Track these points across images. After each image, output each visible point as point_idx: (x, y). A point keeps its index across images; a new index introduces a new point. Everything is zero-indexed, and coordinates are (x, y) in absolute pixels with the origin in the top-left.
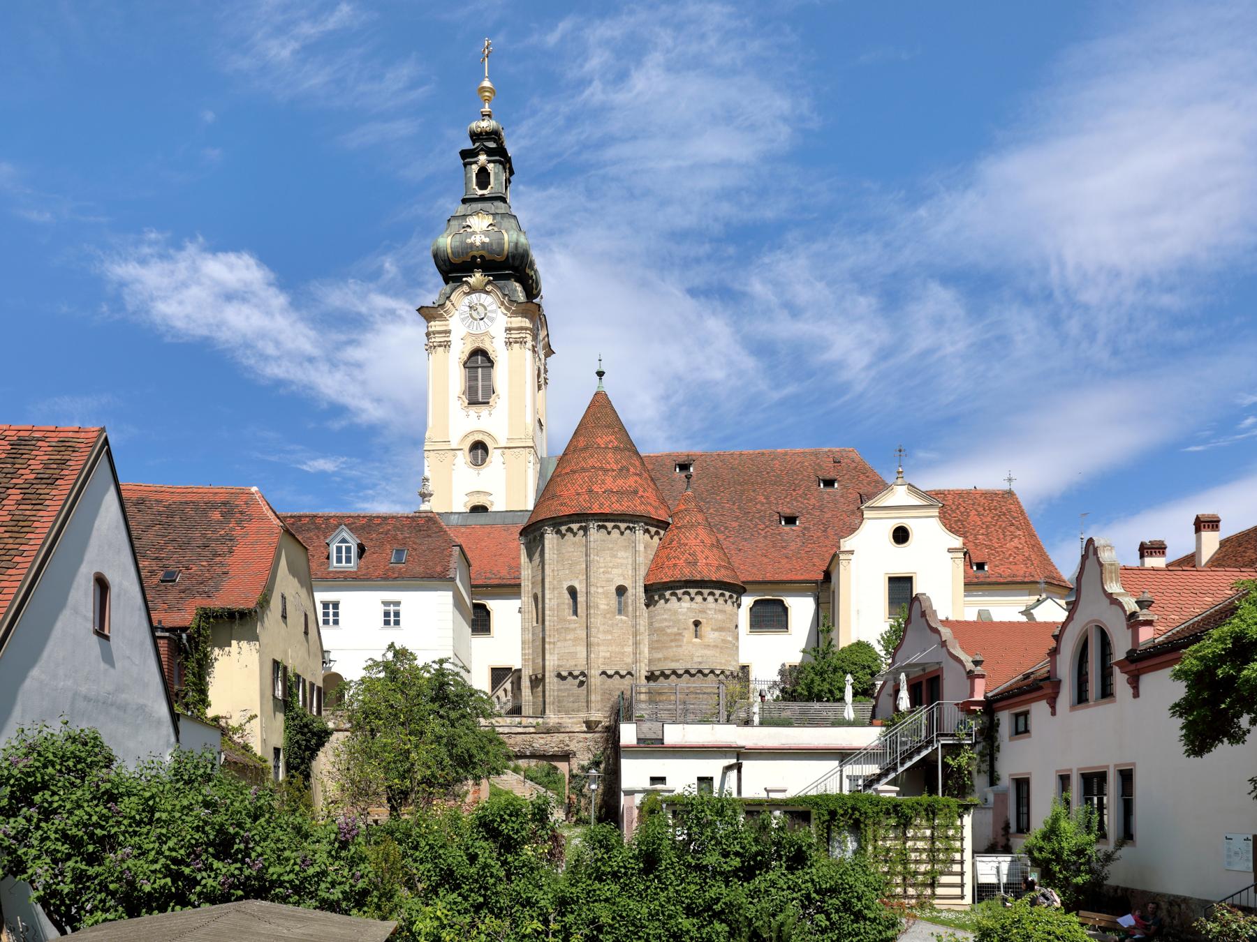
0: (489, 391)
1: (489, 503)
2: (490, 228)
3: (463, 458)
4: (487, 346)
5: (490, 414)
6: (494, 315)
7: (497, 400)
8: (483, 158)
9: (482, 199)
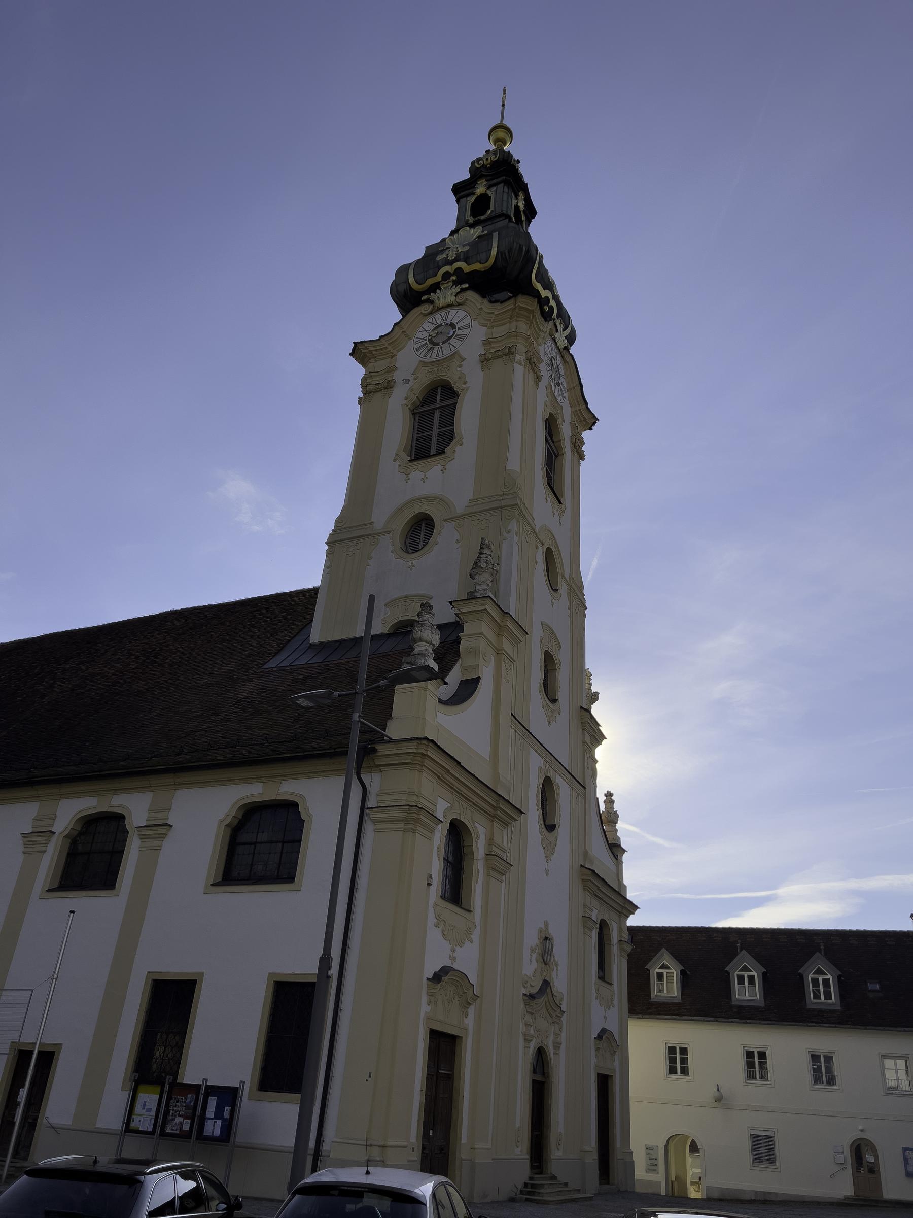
0: (448, 436)
5: (443, 471)
6: (466, 331)
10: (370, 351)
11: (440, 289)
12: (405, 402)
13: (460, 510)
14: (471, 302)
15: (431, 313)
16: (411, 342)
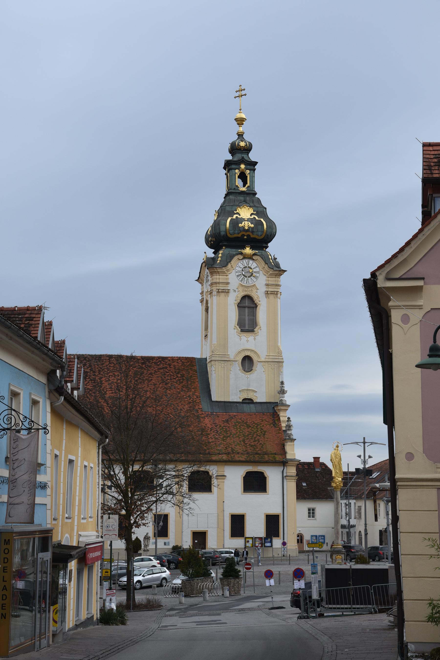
1: (255, 397)
2: (253, 216)
3: (237, 366)
4: (254, 295)
5: (255, 339)
6: (258, 275)
7: (259, 331)
9: (243, 193)
10: (218, 271)
11: (246, 248)
12: (235, 302)
13: (263, 359)
14: (259, 260)
15: (242, 259)
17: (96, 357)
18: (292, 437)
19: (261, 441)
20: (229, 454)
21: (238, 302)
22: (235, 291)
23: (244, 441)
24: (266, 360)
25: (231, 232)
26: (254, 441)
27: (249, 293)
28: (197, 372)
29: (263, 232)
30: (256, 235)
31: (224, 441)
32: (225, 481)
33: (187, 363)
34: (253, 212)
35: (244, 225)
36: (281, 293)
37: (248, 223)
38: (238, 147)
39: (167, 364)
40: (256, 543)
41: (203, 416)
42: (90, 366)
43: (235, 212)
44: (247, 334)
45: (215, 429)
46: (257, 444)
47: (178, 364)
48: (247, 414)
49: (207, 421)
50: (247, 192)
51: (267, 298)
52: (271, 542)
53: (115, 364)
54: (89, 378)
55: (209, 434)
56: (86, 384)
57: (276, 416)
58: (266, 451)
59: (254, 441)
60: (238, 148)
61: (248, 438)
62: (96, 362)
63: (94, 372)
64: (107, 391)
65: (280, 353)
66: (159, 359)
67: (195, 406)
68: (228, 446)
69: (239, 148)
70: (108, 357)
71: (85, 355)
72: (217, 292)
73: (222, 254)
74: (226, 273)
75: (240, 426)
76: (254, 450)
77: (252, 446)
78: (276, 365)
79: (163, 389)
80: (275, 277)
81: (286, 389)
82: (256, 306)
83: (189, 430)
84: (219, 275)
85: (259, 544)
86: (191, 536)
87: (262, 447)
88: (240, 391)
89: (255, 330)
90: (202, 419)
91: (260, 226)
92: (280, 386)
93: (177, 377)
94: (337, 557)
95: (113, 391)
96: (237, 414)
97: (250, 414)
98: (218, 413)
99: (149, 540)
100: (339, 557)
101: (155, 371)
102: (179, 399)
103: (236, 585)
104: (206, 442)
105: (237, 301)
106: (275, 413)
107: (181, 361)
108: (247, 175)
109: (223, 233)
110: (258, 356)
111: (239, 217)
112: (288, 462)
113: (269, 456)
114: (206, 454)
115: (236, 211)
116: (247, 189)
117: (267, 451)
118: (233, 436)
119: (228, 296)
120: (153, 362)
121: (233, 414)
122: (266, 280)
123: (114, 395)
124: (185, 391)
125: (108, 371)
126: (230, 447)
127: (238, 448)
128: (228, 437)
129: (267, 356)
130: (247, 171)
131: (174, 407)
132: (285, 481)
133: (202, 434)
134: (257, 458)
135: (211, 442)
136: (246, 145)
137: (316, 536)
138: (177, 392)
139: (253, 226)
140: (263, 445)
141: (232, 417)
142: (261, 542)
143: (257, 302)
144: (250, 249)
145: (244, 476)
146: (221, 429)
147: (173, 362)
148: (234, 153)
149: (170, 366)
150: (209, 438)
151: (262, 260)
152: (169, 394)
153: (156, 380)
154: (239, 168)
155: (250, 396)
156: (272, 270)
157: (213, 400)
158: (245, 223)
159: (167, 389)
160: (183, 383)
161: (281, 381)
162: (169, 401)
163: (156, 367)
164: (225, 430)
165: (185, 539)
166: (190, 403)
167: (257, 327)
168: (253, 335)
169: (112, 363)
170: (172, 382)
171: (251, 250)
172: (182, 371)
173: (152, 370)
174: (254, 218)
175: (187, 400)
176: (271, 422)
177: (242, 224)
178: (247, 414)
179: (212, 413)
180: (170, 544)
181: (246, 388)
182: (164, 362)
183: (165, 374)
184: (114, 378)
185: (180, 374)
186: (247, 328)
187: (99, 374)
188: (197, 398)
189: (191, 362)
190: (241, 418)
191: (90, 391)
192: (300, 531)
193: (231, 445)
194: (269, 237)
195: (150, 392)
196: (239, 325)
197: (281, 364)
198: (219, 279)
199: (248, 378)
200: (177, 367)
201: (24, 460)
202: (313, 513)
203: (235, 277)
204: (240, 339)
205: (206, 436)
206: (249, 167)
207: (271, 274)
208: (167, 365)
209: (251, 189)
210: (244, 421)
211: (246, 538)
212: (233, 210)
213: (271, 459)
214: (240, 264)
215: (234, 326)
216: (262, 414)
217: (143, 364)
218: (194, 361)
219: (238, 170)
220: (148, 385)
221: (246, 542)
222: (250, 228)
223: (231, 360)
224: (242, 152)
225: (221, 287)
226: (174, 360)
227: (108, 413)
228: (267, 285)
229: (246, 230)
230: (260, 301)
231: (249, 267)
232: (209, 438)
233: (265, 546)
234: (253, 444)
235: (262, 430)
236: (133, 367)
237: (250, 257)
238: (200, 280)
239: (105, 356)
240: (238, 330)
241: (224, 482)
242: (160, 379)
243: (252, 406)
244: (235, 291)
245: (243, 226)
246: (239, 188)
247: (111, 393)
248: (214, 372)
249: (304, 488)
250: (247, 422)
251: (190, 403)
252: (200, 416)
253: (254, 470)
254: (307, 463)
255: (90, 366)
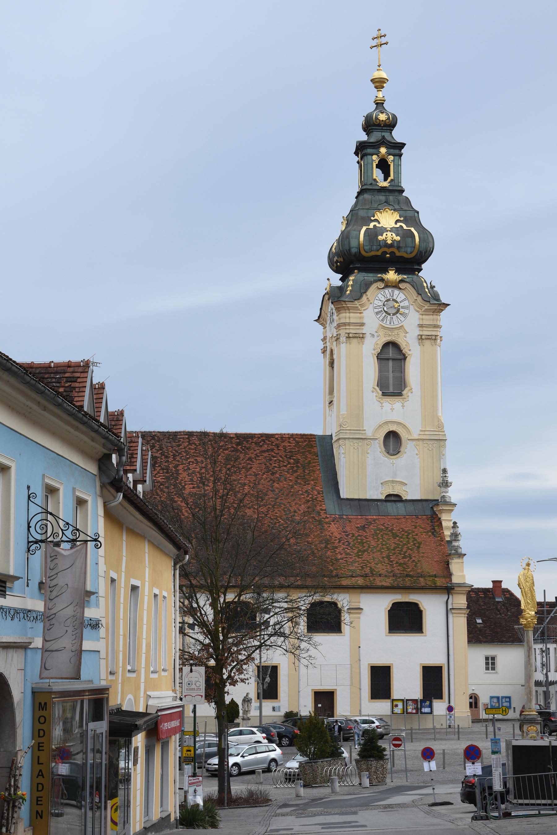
3: (378, 447)
5: (403, 406)
6: (407, 311)
7: (410, 394)
8: (383, 150)
10: (348, 307)
11: (388, 272)
12: (373, 352)
13: (415, 436)
16: (371, 306)
17: (170, 435)
18: (459, 551)
19: (414, 557)
20: (366, 576)
21: (378, 352)
22: (373, 335)
23: (388, 557)
24: (420, 438)
25: (366, 248)
26: (403, 558)
27: (394, 339)
28: (317, 456)
29: (414, 247)
30: (404, 252)
31: (359, 558)
32: (361, 616)
33: (302, 442)
34: (399, 218)
35: (386, 238)
36: (441, 337)
37: (392, 235)
38: (377, 122)
39: (273, 444)
40: (408, 707)
41: (327, 520)
42: (161, 448)
43: (372, 218)
44: (391, 400)
45: (346, 540)
46: (408, 561)
47: (289, 444)
48: (392, 517)
49: (333, 528)
50: (390, 188)
51: (421, 345)
52: (431, 706)
53: (197, 446)
54: (159, 466)
55: (336, 547)
56: (156, 475)
57: (435, 521)
58: (422, 572)
59: (403, 558)
60: (375, 123)
61: (395, 553)
62: (170, 442)
63: (167, 457)
64: (185, 485)
65: (440, 427)
66: (261, 437)
67: (316, 506)
68: (365, 565)
69: (377, 124)
70: (186, 435)
71: (154, 432)
72: (347, 337)
73: (353, 280)
74: (359, 310)
75: (382, 536)
76: (403, 571)
77: (400, 565)
78: (434, 445)
79: (268, 482)
80: (433, 315)
81: (450, 480)
82: (405, 358)
83: (308, 542)
84: (350, 313)
85: (413, 709)
86: (312, 698)
87: (415, 566)
88: (382, 484)
89: (404, 393)
90: (326, 526)
91: (410, 239)
92: (442, 475)
93: (289, 463)
94: (529, 728)
95: (194, 484)
96: (377, 517)
97: (397, 517)
98: (349, 517)
99: (250, 703)
100: (533, 729)
101: (256, 454)
102: (292, 495)
103: (380, 769)
104: (332, 559)
105: (376, 351)
106: (434, 516)
107: (294, 439)
108: (389, 163)
109: (354, 250)
110: (409, 431)
111: (378, 225)
112: (454, 589)
113: (425, 580)
114: (333, 577)
115: (374, 217)
116: (389, 184)
117: (423, 572)
118: (372, 550)
119: (363, 344)
120: (252, 442)
121: (372, 517)
122: (419, 319)
123: (197, 491)
124: (300, 484)
125: (187, 455)
126: (369, 567)
127: (381, 568)
128: (365, 551)
129: (421, 431)
130: (390, 156)
131: (284, 508)
132: (450, 616)
133: (326, 547)
134: (408, 582)
135: (339, 559)
136: (389, 118)
137: (498, 698)
138: (289, 485)
139: (398, 238)
140: (416, 563)
141: (370, 522)
142: (416, 706)
143: (406, 353)
144: (395, 273)
145: (389, 608)
146: (353, 541)
147: (283, 442)
148: (371, 131)
149: (278, 447)
150: (337, 554)
151: (413, 289)
152: (277, 488)
153: (258, 468)
154: (378, 152)
155: (397, 491)
156: (428, 305)
157: (342, 497)
158: (387, 235)
159: (274, 481)
160: (297, 472)
161: (442, 468)
162: (277, 498)
163: (258, 449)
164: (360, 541)
165: (302, 702)
166: (308, 501)
167: (407, 389)
168: (401, 400)
169: (193, 443)
170: (281, 470)
171: (397, 274)
172: (297, 454)
173: (252, 453)
174: (401, 226)
175: (304, 498)
176: (429, 528)
177: (382, 236)
178: (392, 517)
179: (341, 517)
180: (281, 710)
181: (391, 479)
182: (270, 441)
183: (271, 460)
184: (196, 466)
185: (293, 459)
186: (391, 390)
187: (175, 459)
188: (319, 493)
189: (310, 441)
190: (384, 523)
191: (161, 484)
192: (473, 690)
193: (369, 563)
194: (423, 254)
195: (250, 486)
196: (379, 386)
197: (442, 443)
198: (350, 318)
199: (393, 464)
200: (289, 448)
201: (66, 586)
202: (493, 664)
203: (374, 315)
204: (382, 407)
205: (332, 551)
206: (392, 151)
207: (426, 310)
208: (274, 445)
209: (396, 184)
210: (388, 528)
211: (393, 700)
212: (369, 215)
213: (429, 583)
214: (380, 296)
215: (372, 387)
216: (414, 517)
217: (238, 444)
218: (313, 439)
219: (376, 156)
220: (246, 475)
221: (393, 706)
222: (395, 242)
223: (367, 437)
224: (382, 129)
225: (353, 330)
226: (284, 439)
227: (188, 517)
228: (421, 326)
229: (389, 244)
230: (410, 350)
231: (394, 300)
232: (337, 554)
233: (422, 713)
234: (402, 561)
235: (416, 540)
236: (224, 450)
237: (396, 286)
238: (320, 319)
239: (182, 434)
240: (378, 393)
241: (359, 618)
242: (263, 466)
243: (400, 505)
244: (373, 335)
245: (384, 240)
246: (377, 182)
247: (192, 488)
248: (343, 456)
249: (479, 626)
250: (392, 529)
251: (308, 501)
252: (323, 521)
253: (404, 601)
254: (482, 589)
255: (161, 448)
